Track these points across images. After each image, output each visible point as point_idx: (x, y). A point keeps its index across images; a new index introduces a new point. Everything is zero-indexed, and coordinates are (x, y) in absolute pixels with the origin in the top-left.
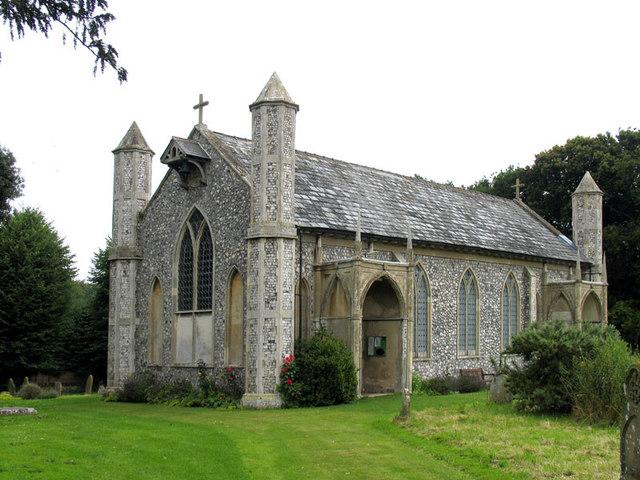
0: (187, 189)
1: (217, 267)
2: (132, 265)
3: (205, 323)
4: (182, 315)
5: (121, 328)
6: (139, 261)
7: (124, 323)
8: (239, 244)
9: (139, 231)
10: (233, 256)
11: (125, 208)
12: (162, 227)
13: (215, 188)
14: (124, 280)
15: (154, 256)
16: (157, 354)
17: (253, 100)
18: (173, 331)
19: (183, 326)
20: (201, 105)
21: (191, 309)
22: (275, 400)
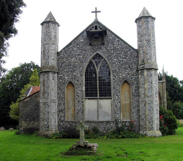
0: (90, 45)
1: (114, 79)
2: (56, 75)
3: (106, 104)
4: (89, 99)
5: (52, 104)
6: (58, 73)
7: (53, 101)
8: (128, 71)
9: (58, 60)
10: (124, 75)
11: (52, 48)
12: (73, 59)
13: (110, 47)
14: (53, 81)
15: (68, 72)
16: (70, 116)
17: (137, 17)
18: (83, 106)
19: (90, 105)
20: (96, 12)
21: (97, 96)
22: (159, 133)
